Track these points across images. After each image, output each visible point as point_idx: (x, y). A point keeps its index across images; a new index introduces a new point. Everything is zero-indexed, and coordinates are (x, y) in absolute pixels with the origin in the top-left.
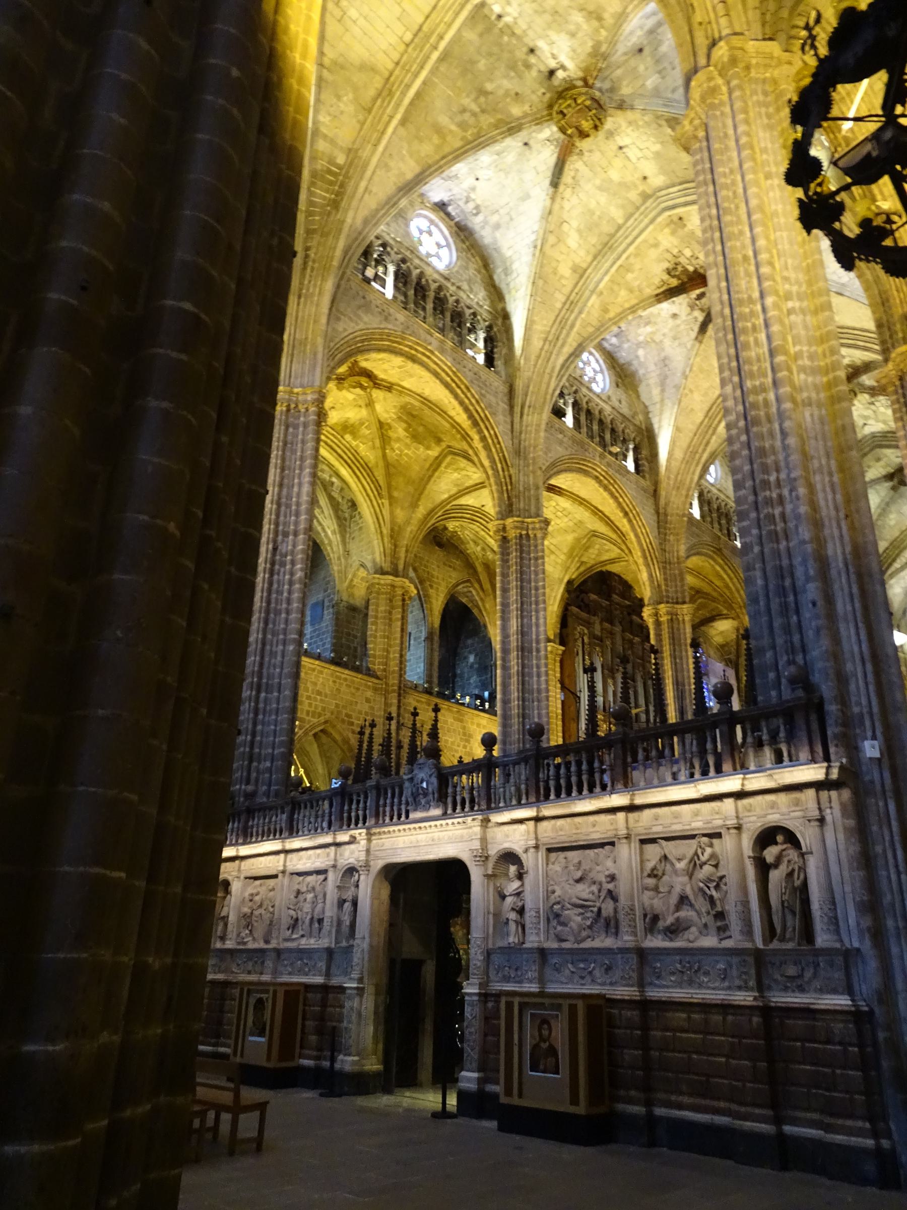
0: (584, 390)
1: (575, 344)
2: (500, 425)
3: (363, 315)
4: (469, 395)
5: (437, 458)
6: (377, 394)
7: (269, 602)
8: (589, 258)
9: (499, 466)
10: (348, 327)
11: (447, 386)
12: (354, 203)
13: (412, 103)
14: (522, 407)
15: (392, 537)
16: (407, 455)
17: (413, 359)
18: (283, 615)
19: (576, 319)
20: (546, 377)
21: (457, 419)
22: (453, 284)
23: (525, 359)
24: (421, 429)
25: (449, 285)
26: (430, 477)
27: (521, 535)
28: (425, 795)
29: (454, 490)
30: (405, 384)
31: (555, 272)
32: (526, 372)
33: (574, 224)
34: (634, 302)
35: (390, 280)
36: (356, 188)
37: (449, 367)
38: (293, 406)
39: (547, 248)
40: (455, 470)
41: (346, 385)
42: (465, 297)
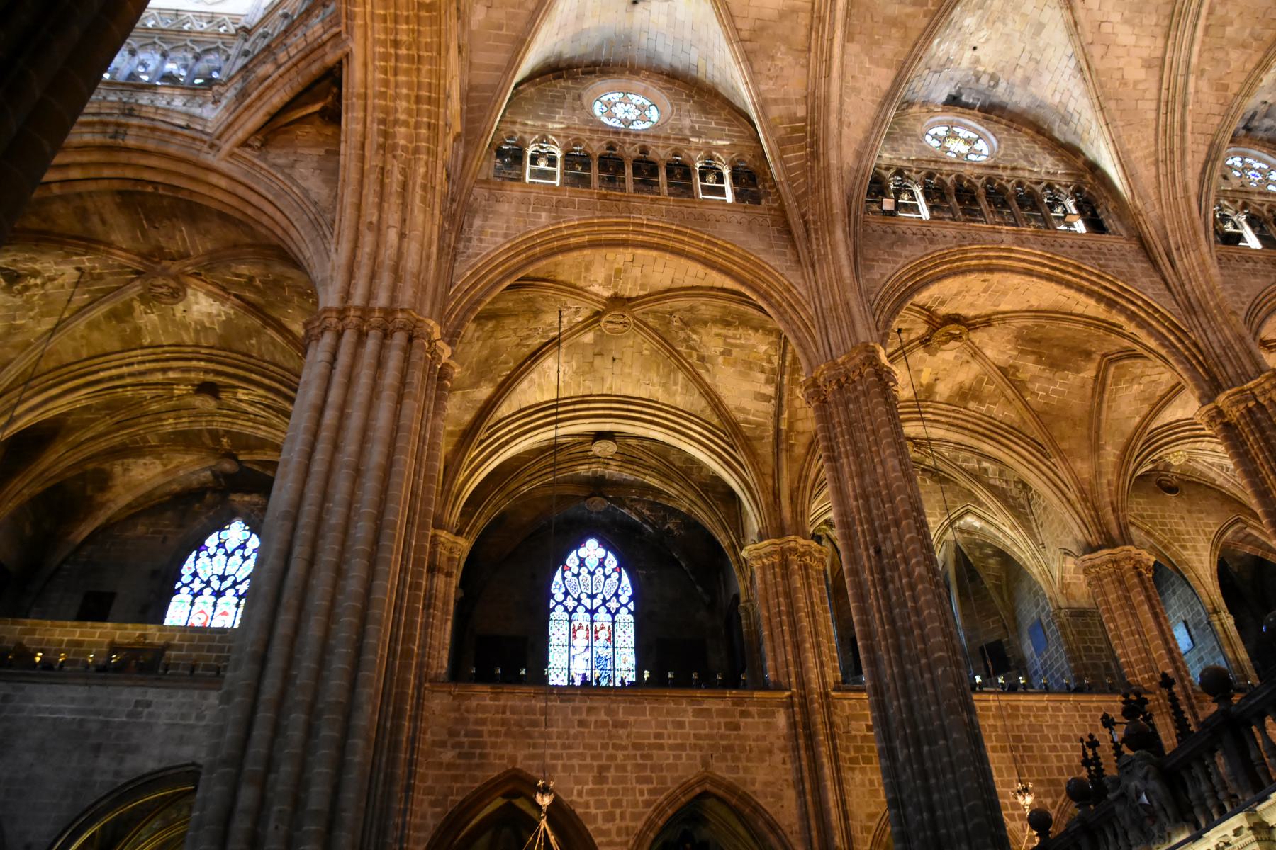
0: (1257, 198)
1: (1204, 149)
2: (1148, 289)
3: (899, 251)
4: (1084, 274)
5: (1097, 376)
6: (978, 337)
7: (893, 622)
8: (1160, 42)
9: (1172, 338)
10: (886, 271)
11: (1049, 278)
12: (833, 142)
13: (848, 15)
14: (1169, 255)
15: (1085, 500)
16: (1053, 391)
17: (990, 269)
18: (917, 632)
19: (1183, 116)
20: (1181, 202)
21: (1089, 312)
22: (1005, 168)
23: (1140, 197)
24: (1056, 352)
25: (1000, 172)
26: (1100, 404)
27: (1249, 410)
28: (1153, 817)
29: (1146, 408)
30: (1003, 307)
31: (1124, 82)
32: (1151, 213)
33: (1116, 17)
34: (1257, 57)
35: (921, 202)
36: (827, 126)
37: (1041, 256)
38: (843, 380)
39: (1097, 63)
40: (1132, 381)
41: (935, 344)
42: (1027, 174)
